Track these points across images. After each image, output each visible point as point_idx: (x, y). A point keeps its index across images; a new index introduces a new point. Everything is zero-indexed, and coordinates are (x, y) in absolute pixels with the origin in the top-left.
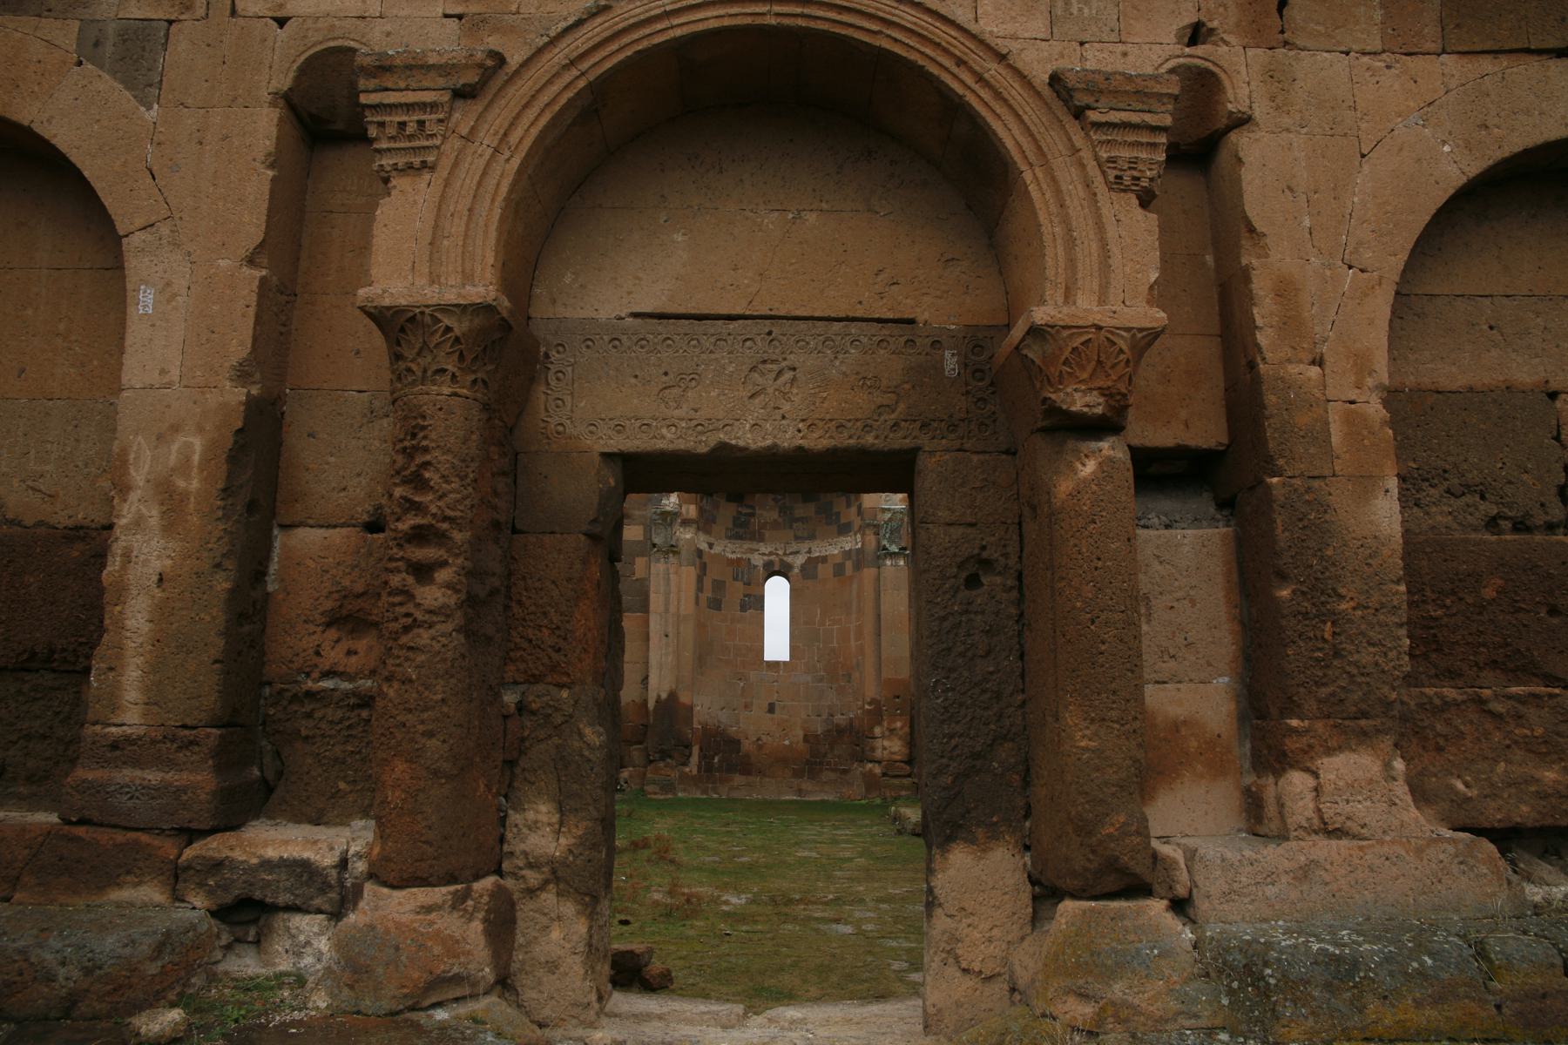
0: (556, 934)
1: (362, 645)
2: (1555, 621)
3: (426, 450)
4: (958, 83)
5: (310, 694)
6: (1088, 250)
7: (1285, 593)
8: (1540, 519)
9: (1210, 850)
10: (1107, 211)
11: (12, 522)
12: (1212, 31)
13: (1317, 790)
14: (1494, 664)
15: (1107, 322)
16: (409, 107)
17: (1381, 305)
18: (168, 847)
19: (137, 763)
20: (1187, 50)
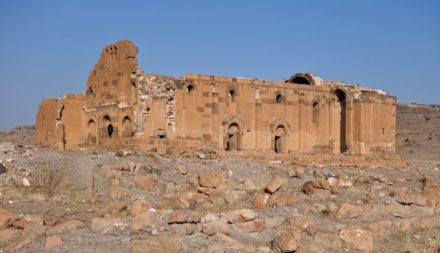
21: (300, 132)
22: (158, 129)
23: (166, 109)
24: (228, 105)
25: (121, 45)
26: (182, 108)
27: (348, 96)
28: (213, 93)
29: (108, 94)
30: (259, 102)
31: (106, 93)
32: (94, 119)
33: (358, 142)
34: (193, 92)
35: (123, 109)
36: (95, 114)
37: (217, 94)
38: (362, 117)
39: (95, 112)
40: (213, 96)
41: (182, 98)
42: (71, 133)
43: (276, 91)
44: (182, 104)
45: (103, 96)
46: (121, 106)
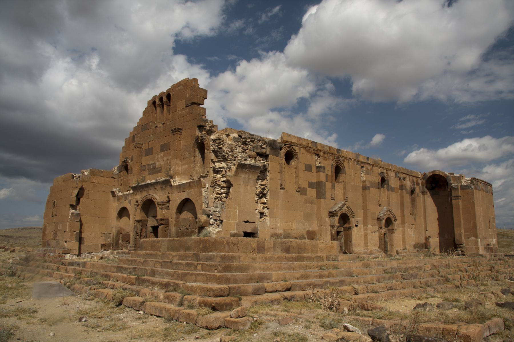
21: (403, 227)
22: (245, 222)
23: (257, 187)
24: (335, 187)
25: (179, 88)
26: (279, 188)
27: (452, 182)
28: (318, 167)
29: (152, 166)
30: (368, 185)
31: (149, 165)
32: (128, 206)
33: (473, 238)
34: (293, 163)
37: (324, 168)
38: (476, 207)
39: (130, 196)
40: (319, 171)
41: (279, 170)
42: (92, 227)
43: (380, 172)
44: (279, 181)
45: (145, 170)
46: (176, 181)
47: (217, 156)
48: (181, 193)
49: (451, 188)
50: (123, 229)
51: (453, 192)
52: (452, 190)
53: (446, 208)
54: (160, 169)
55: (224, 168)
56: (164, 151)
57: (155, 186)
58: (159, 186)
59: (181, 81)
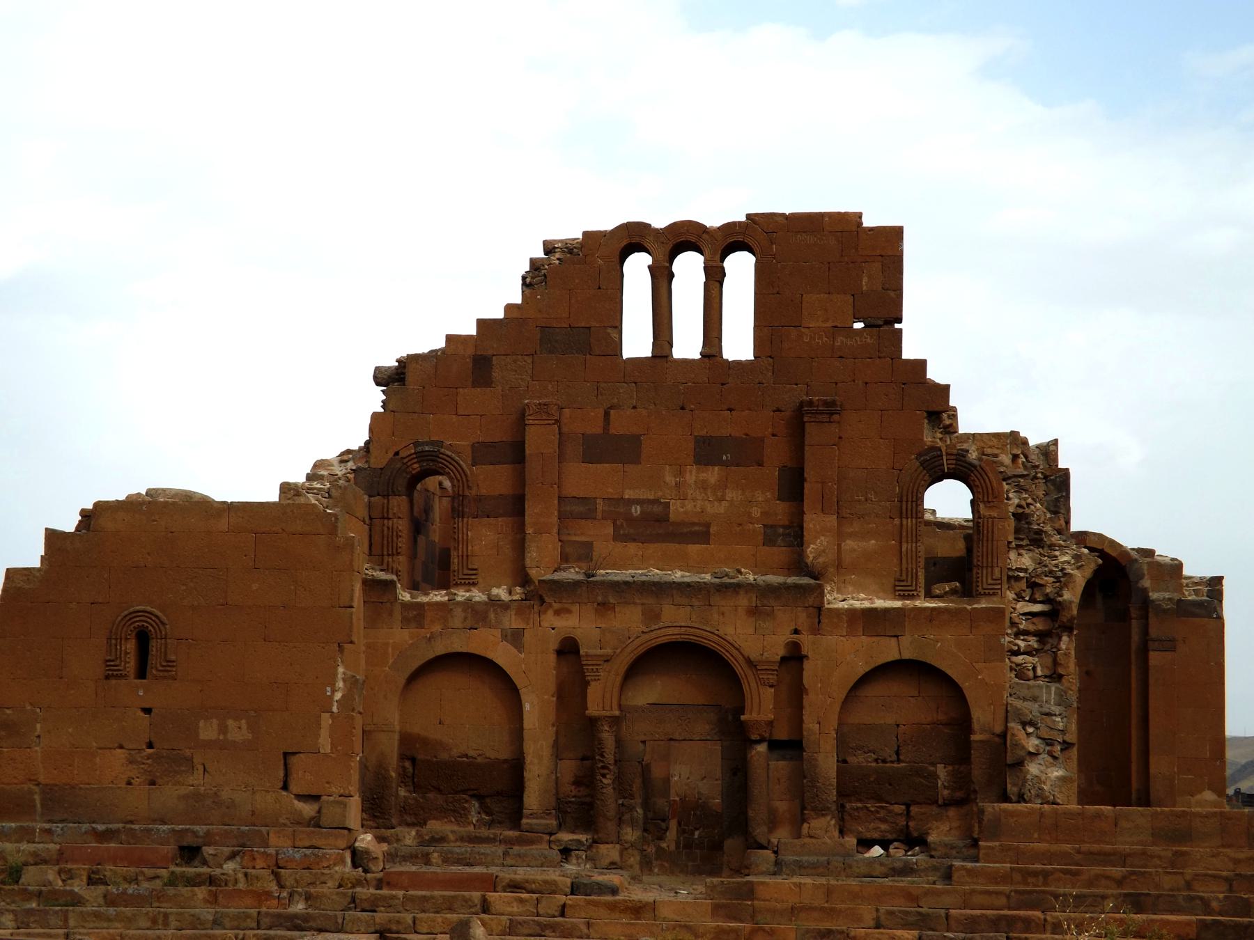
0: (632, 859)
1: (582, 789)
2: (890, 787)
3: (603, 748)
4: (727, 656)
5: (570, 802)
6: (756, 700)
7: (805, 781)
8: (889, 759)
9: (783, 841)
10: (761, 691)
11: (487, 758)
12: (800, 631)
13: (809, 827)
14: (873, 798)
15: (759, 719)
16: (593, 665)
17: (837, 708)
18: (546, 837)
19: (537, 818)
20: (792, 636)
27: (1146, 583)
29: (636, 510)
32: (502, 655)
35: (871, 620)
36: (511, 621)
45: (589, 515)
47: (1017, 531)
48: (874, 639)
49: (1146, 603)
50: (425, 742)
51: (1152, 620)
52: (1151, 615)
53: (1088, 673)
54: (697, 528)
55: (1026, 570)
56: (726, 464)
57: (716, 599)
58: (743, 601)
59: (822, 215)
